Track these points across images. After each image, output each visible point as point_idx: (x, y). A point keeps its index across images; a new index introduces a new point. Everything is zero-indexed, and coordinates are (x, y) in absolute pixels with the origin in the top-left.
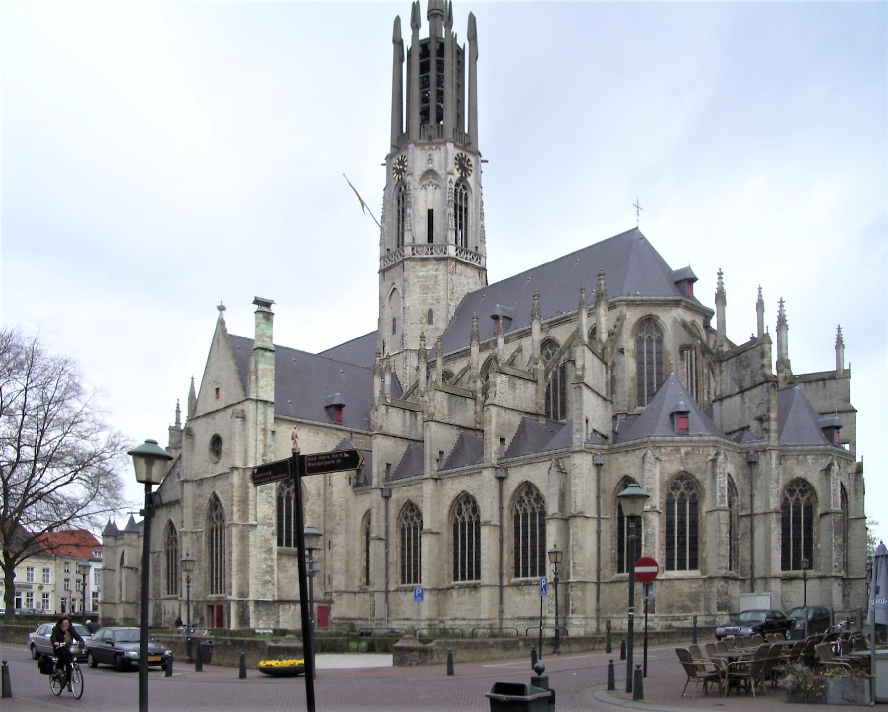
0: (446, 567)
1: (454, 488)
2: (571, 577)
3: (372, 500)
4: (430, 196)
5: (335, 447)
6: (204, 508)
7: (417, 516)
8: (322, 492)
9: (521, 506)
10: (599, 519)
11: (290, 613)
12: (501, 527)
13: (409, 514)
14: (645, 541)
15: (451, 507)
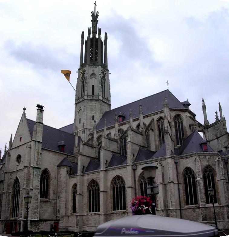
0: (110, 205)
1: (112, 174)
2: (171, 207)
3: (77, 180)
4: (93, 81)
5: (61, 160)
6: (12, 183)
7: (96, 185)
8: (57, 177)
9: (143, 180)
10: (178, 184)
11: (44, 225)
12: (135, 188)
13: (93, 185)
14: (200, 192)
15: (112, 181)
